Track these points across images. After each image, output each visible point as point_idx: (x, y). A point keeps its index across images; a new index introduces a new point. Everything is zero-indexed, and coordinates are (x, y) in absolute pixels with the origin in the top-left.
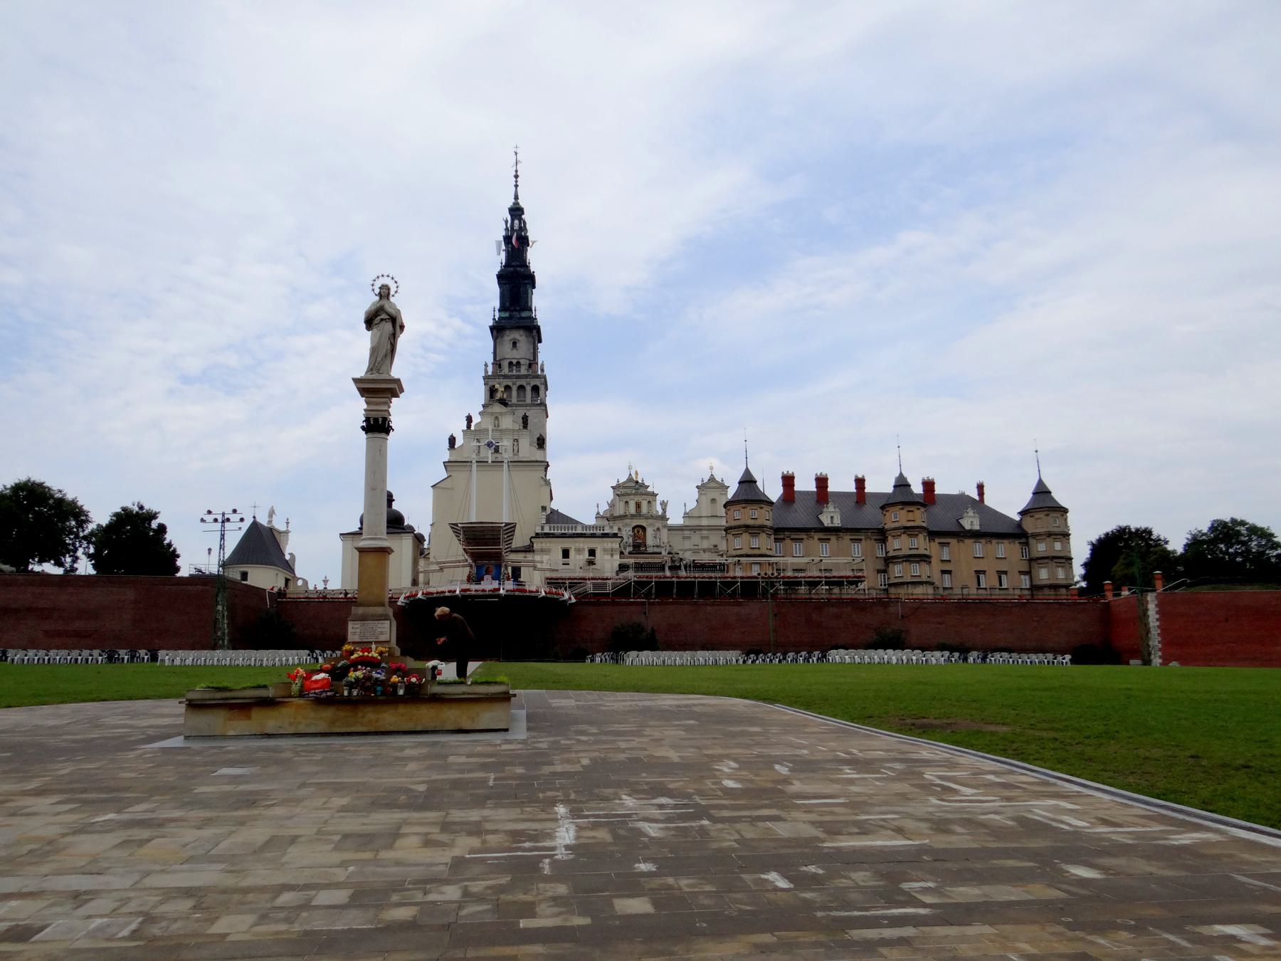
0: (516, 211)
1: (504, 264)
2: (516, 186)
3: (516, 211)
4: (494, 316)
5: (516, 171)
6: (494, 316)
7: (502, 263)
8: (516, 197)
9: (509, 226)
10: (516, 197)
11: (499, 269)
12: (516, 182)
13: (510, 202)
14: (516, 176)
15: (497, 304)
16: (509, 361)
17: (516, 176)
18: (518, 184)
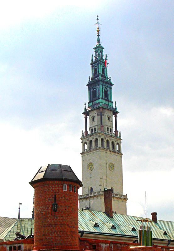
0: (99, 49)
1: (91, 78)
2: (98, 36)
3: (99, 49)
4: (85, 107)
5: (98, 28)
6: (85, 107)
7: (89, 78)
8: (99, 41)
9: (94, 59)
10: (99, 41)
11: (88, 81)
12: (98, 33)
13: (96, 44)
14: (98, 31)
15: (87, 101)
16: (91, 128)
17: (98, 31)
18: (99, 34)
